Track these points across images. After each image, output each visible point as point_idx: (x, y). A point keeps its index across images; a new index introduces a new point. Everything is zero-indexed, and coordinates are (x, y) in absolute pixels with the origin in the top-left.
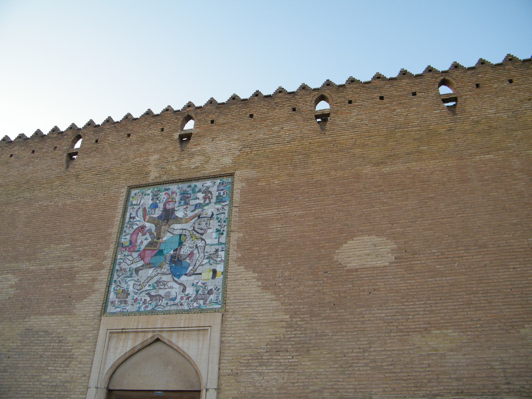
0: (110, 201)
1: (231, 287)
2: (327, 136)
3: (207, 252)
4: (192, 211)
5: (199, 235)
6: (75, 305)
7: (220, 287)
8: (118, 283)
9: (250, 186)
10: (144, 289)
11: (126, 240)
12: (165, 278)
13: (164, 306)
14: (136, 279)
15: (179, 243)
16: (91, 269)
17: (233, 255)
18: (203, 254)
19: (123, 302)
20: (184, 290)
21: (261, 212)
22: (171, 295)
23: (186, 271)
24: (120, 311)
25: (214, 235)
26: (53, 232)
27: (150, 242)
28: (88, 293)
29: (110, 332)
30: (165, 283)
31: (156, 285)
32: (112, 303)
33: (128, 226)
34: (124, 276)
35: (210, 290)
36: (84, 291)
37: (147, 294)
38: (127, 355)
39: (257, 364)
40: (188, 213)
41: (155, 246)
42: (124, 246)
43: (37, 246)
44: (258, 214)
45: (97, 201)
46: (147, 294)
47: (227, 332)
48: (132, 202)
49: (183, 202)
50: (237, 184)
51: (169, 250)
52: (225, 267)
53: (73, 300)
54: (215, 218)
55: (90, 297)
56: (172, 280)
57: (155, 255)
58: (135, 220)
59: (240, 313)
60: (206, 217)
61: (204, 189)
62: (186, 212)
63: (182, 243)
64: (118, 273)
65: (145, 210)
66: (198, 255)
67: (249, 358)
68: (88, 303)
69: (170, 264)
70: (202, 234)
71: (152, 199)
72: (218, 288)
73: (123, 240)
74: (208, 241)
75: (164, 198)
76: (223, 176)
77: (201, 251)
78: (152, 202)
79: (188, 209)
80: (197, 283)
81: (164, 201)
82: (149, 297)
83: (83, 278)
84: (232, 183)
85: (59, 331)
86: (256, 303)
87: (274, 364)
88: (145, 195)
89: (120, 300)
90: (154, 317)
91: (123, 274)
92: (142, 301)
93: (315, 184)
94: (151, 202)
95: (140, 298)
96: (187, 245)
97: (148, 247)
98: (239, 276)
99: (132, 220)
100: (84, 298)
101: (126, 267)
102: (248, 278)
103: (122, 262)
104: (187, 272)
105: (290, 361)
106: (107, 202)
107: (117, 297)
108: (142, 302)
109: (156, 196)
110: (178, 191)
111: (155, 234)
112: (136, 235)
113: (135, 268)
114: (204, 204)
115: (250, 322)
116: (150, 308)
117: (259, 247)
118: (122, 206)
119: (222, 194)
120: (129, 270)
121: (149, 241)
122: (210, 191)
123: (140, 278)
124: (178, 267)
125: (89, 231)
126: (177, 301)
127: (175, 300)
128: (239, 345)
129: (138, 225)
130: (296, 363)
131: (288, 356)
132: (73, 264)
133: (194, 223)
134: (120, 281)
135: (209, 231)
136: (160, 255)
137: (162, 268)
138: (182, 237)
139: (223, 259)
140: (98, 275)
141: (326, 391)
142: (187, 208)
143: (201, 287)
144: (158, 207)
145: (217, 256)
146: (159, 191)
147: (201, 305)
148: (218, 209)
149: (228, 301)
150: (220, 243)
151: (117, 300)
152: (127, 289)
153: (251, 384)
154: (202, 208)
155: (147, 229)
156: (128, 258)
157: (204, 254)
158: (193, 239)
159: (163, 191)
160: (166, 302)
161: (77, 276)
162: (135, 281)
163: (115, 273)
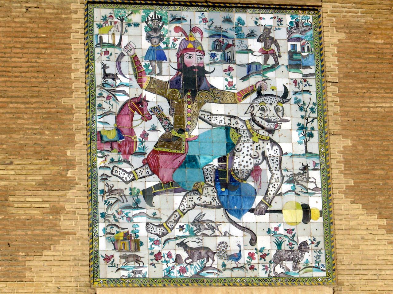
0: (46, 28)
1: (344, 242)
3: (286, 170)
4: (244, 79)
5: (266, 134)
6: (25, 261)
8: (112, 219)
9: (356, 43)
10: (171, 234)
11: (107, 127)
12: (211, 215)
13: (218, 270)
14: (150, 212)
15: (228, 145)
16: (43, 185)
18: (279, 173)
19: (131, 259)
20: (253, 241)
21: (380, 101)
22: (228, 248)
23: (252, 204)
24: (129, 277)
25: (296, 136)
27: (162, 136)
28: (49, 238)
30: (213, 225)
31: (195, 228)
32: (107, 259)
33: (105, 94)
35: (302, 243)
36: (38, 232)
37: (180, 244)
40: (235, 81)
41: (178, 147)
42: (105, 139)
45: (13, 25)
48: (101, 37)
49: (219, 54)
51: (209, 157)
52: (324, 202)
53: (18, 250)
54: (292, 101)
55: (58, 247)
56: (226, 220)
57: (180, 166)
58: (118, 82)
60: (272, 95)
61: (259, 31)
62: (230, 80)
63: (234, 145)
64: (106, 198)
65: (135, 61)
66: (269, 175)
68: (56, 258)
69: (215, 187)
70: (271, 131)
71: (149, 38)
72: (317, 240)
73: (100, 127)
74: (286, 148)
75: (175, 40)
76: (298, 9)
77: (275, 166)
79: (232, 73)
80: (277, 229)
81: (177, 47)
82: (185, 250)
83: (28, 205)
84: (318, 28)
86: (388, 272)
88: (129, 25)
89: (122, 254)
91: (118, 200)
94: (147, 45)
95: (167, 252)
96: (245, 150)
97: (162, 146)
98: (353, 223)
99: (110, 81)
100: (45, 249)
101: (122, 185)
102: (372, 228)
103: (110, 174)
104: (254, 206)
106: (40, 31)
107: (115, 249)
109: (155, 30)
110: (203, 27)
113: (141, 189)
114: (265, 66)
116: (190, 272)
117: (383, 169)
118: (83, 46)
119: (299, 49)
120: (131, 194)
122: (272, 39)
123: (157, 212)
124: (234, 194)
125: (12, 97)
126: (244, 260)
129: (127, 94)
133: (251, 106)
134: (115, 216)
135: (285, 126)
136: (192, 167)
137: (201, 194)
138: (231, 134)
139: (319, 186)
140: (62, 199)
142: (230, 69)
143: (285, 236)
144: (165, 59)
145: (308, 178)
146: (160, 19)
147: (289, 270)
148: (295, 82)
149: (340, 267)
150: (308, 155)
151: (117, 255)
152: (132, 231)
154: (263, 75)
157: (281, 173)
158: (256, 138)
159: (171, 22)
160: (221, 262)
161: (11, 199)
162: (149, 217)
163: (100, 198)
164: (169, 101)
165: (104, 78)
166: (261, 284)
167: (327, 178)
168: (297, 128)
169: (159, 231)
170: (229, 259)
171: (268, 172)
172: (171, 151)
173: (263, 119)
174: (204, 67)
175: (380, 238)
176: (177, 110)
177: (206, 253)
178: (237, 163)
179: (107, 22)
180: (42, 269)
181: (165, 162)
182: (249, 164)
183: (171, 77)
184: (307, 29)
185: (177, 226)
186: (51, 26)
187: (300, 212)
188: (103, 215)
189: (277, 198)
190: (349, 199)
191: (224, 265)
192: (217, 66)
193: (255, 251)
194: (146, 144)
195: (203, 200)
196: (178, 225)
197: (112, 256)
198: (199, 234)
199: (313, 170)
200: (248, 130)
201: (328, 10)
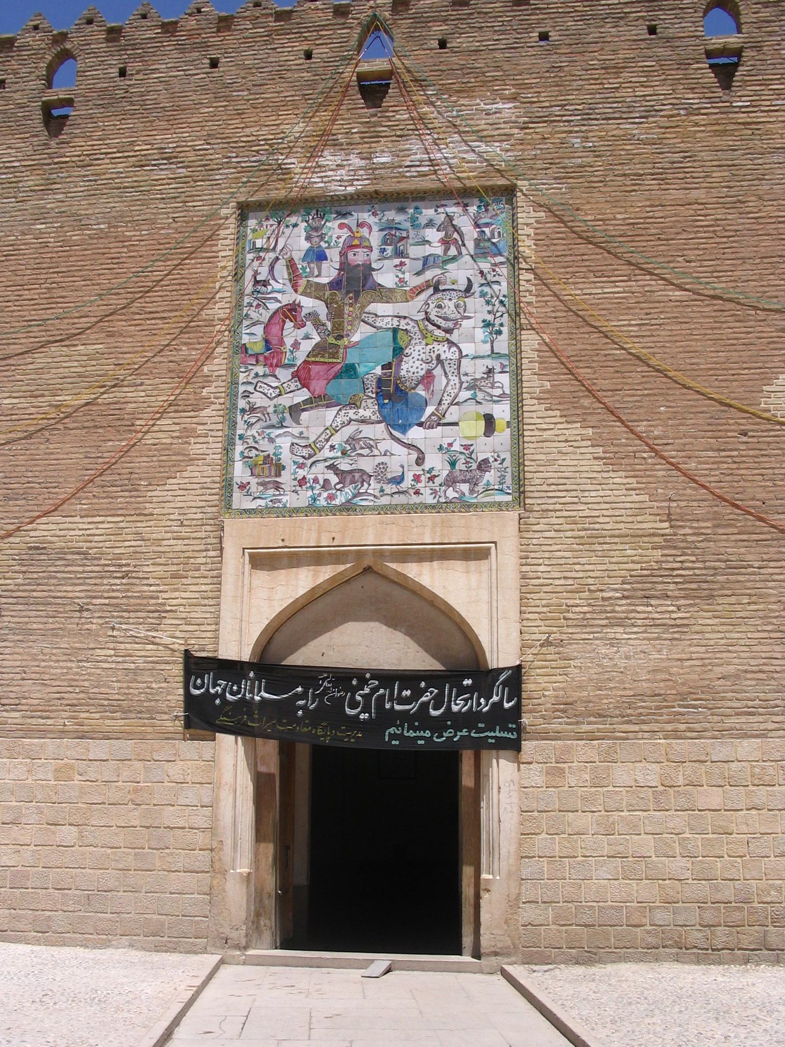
2: (737, 110)
3: (466, 374)
4: (418, 274)
7: (507, 455)
8: (250, 441)
10: (320, 456)
12: (368, 431)
15: (394, 350)
17: (532, 383)
18: (457, 379)
19: (271, 486)
20: (420, 461)
21: (588, 286)
22: (388, 470)
24: (266, 507)
25: (480, 334)
26: (49, 311)
29: (249, 553)
30: (371, 442)
31: (348, 448)
32: (242, 487)
34: (261, 424)
37: (328, 467)
38: (299, 605)
39: (604, 622)
40: (407, 276)
42: (250, 352)
43: (12, 347)
44: (582, 289)
46: (328, 467)
47: (532, 555)
48: (254, 243)
49: (389, 249)
50: (524, 215)
54: (477, 295)
55: (185, 474)
56: (387, 436)
58: (270, 288)
59: (558, 514)
60: (453, 290)
62: (401, 276)
63: (402, 349)
64: (246, 417)
66: (444, 381)
67: (586, 609)
69: (377, 399)
70: (449, 331)
71: (308, 238)
73: (245, 339)
74: (467, 348)
75: (339, 237)
78: (309, 245)
80: (450, 445)
81: (341, 245)
82: (336, 474)
85: (117, 551)
86: (593, 494)
87: (639, 622)
90: (355, 520)
92: (318, 483)
93: (711, 229)
94: (306, 245)
95: (313, 476)
96: (415, 354)
98: (546, 434)
102: (573, 439)
103: (252, 391)
104: (423, 420)
105: (674, 616)
107: (252, 475)
108: (318, 486)
109: (316, 229)
111: (329, 325)
112: (278, 327)
114: (446, 258)
115: (582, 533)
116: (340, 500)
120: (275, 412)
121: (314, 342)
122: (454, 226)
123: (304, 430)
124: (399, 406)
125: (151, 313)
127: (399, 483)
128: (562, 582)
129: (279, 301)
130: (685, 622)
131: (668, 606)
132: (124, 395)
135: (465, 323)
139: (507, 391)
140: (195, 420)
141: (749, 676)
142: (402, 264)
143: (461, 453)
144: (326, 259)
148: (482, 273)
150: (493, 354)
151: (254, 481)
152: (274, 454)
153: (592, 662)
155: (304, 312)
156: (266, 381)
157: (460, 379)
158: (430, 340)
160: (378, 486)
163: (239, 417)
164: (327, 305)
165: (254, 285)
166: (426, 511)
167: (517, 381)
168: (482, 325)
169: (305, 452)
170: (389, 483)
171: (443, 377)
172: (326, 360)
173: (440, 317)
174: (370, 264)
175: (583, 450)
176: (336, 314)
177: (361, 476)
178: (405, 369)
179: (262, 226)
180: (165, 499)
181: (318, 373)
182: (419, 370)
183: (331, 278)
184: (498, 212)
185: (328, 446)
186: (198, 234)
187: (482, 423)
188: (241, 437)
189: (454, 409)
190: (543, 406)
191: (382, 490)
192: (386, 262)
193: (421, 472)
194: (297, 354)
195: (360, 415)
196: (329, 443)
197: (249, 483)
198: (353, 454)
199: (500, 372)
200: (421, 331)
201: (524, 189)
